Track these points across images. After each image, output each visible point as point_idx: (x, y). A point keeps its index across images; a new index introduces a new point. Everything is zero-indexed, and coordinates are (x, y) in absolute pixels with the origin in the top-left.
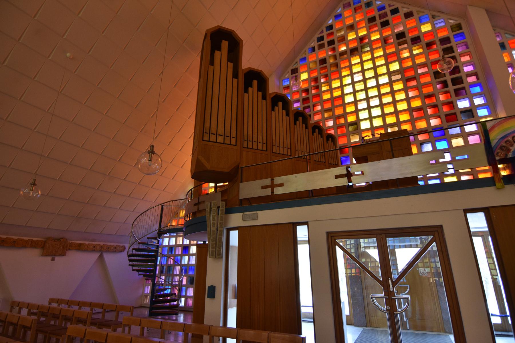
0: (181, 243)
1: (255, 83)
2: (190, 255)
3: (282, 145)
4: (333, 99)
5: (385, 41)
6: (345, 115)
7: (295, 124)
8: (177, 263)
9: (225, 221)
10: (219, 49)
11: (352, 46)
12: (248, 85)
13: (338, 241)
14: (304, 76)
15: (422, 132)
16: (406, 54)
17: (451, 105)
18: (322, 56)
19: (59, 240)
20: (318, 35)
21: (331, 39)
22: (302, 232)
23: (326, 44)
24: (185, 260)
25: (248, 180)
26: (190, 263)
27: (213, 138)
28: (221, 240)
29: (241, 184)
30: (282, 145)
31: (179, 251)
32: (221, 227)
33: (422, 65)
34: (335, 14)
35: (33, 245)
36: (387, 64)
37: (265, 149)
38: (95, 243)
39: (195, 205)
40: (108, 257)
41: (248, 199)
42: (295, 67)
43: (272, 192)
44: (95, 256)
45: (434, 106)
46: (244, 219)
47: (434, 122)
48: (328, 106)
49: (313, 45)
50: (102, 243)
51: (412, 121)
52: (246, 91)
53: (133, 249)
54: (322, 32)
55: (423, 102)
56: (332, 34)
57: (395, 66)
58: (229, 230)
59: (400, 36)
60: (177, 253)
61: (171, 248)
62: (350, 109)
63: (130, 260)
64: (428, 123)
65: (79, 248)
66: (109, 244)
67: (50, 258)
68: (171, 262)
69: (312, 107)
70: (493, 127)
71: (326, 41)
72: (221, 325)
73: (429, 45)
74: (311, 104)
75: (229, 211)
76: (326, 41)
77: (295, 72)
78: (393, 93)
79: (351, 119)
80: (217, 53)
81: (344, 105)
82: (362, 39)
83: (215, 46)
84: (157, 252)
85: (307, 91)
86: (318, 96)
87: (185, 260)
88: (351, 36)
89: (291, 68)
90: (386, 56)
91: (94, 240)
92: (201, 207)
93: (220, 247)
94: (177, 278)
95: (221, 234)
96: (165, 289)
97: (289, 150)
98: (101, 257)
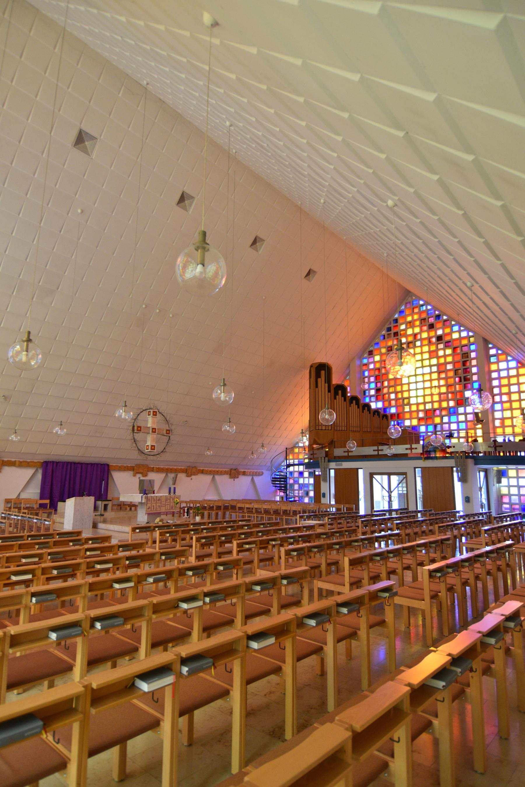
0: (297, 470)
1: (340, 392)
2: (304, 478)
3: (355, 426)
4: (395, 379)
5: (429, 339)
6: (402, 392)
7: (363, 412)
8: (296, 482)
9: (328, 465)
10: (320, 377)
11: (410, 339)
12: (336, 394)
13: (374, 476)
14: (377, 358)
15: (445, 409)
16: (441, 353)
17: (462, 393)
18: (390, 343)
19: (235, 470)
20: (387, 326)
21: (395, 331)
22: (361, 472)
23: (392, 335)
24: (301, 481)
25: (338, 447)
26: (305, 482)
27: (320, 428)
28: (326, 474)
29: (334, 449)
30: (355, 426)
31: (296, 475)
32: (327, 468)
33: (449, 363)
34: (398, 310)
35: (225, 473)
36: (430, 359)
37: (346, 429)
38: (249, 471)
39: (311, 454)
40: (256, 478)
41: (339, 457)
42: (371, 349)
43: (348, 454)
44: (250, 478)
45: (452, 393)
46: (336, 465)
47: (452, 404)
48: (392, 383)
49: (384, 332)
50: (253, 471)
51: (440, 401)
52: (335, 398)
53: (275, 475)
54: (390, 324)
55: (447, 389)
56: (397, 326)
57: (434, 361)
58: (330, 470)
59: (439, 338)
60: (295, 476)
61: (291, 473)
62: (405, 388)
63: (273, 481)
64: (448, 404)
65: (244, 473)
66: (256, 471)
67: (232, 479)
68: (291, 481)
69: (381, 382)
70: (426, 438)
71: (392, 332)
72: (329, 503)
73: (455, 349)
74: (381, 381)
75: (329, 461)
76: (392, 332)
77: (371, 353)
78: (431, 380)
79: (406, 395)
80: (319, 380)
81: (402, 385)
82: (415, 335)
83: (318, 376)
84: (286, 476)
85: (379, 369)
86: (387, 374)
87: (301, 481)
88: (410, 332)
89: (368, 350)
90: (430, 352)
91: (249, 469)
92: (315, 456)
93: (326, 477)
94: (297, 492)
95: (327, 471)
96: (292, 498)
97: (359, 428)
98: (253, 479)
